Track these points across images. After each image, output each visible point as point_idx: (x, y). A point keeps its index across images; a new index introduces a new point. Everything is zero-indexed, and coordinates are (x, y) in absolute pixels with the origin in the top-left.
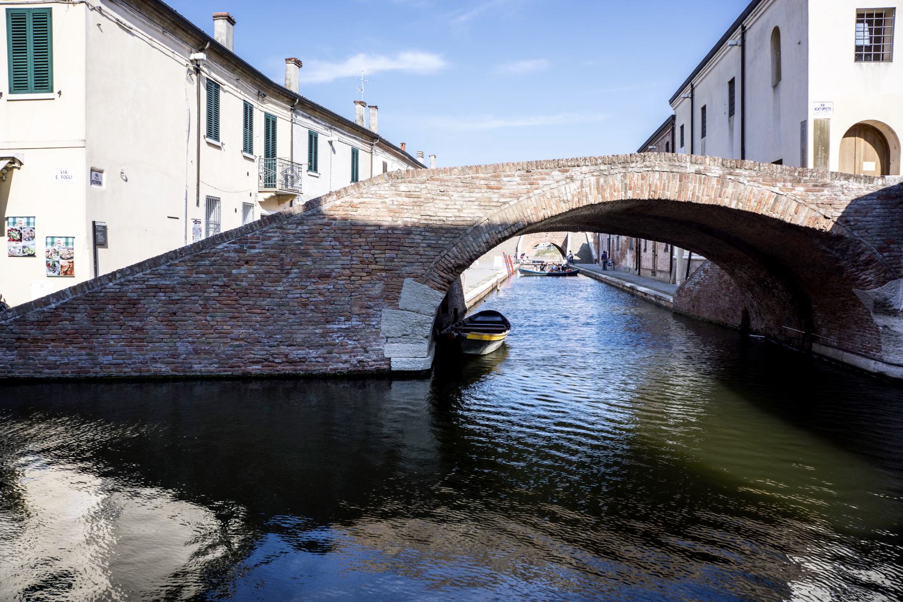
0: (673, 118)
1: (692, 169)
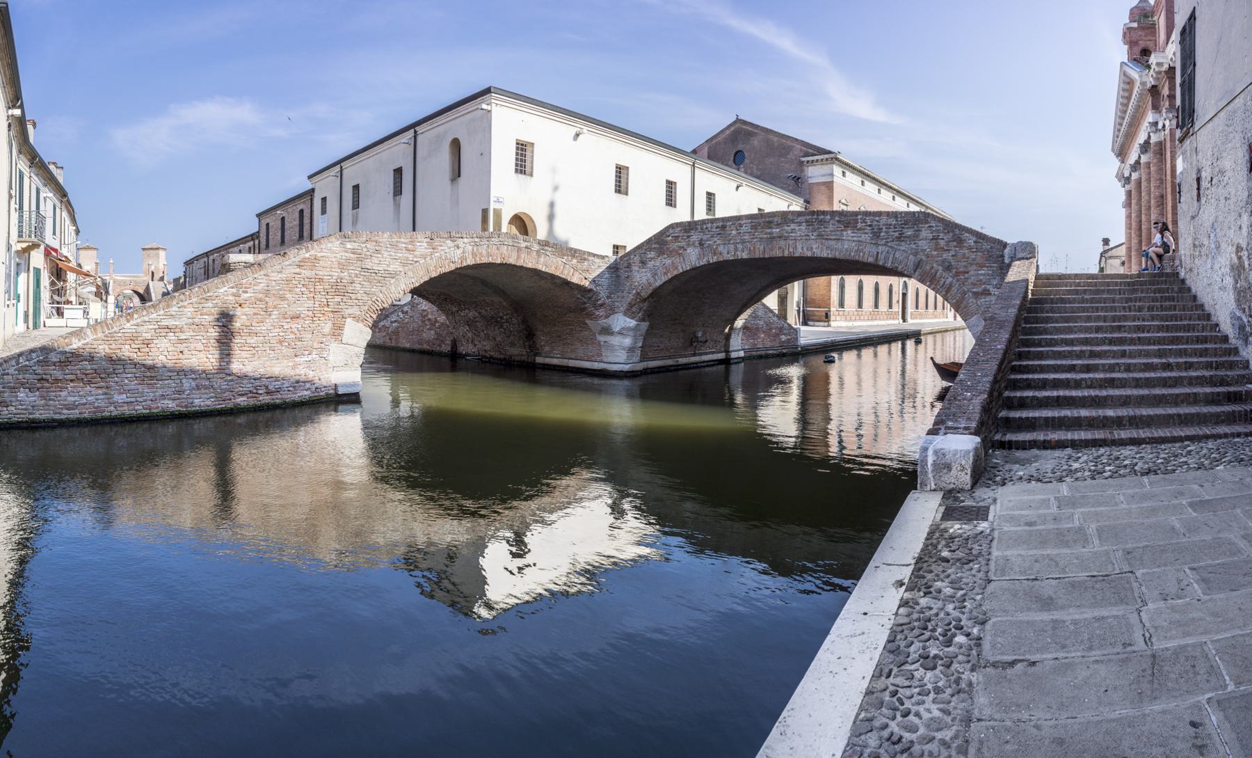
0: (313, 190)
1: (523, 245)
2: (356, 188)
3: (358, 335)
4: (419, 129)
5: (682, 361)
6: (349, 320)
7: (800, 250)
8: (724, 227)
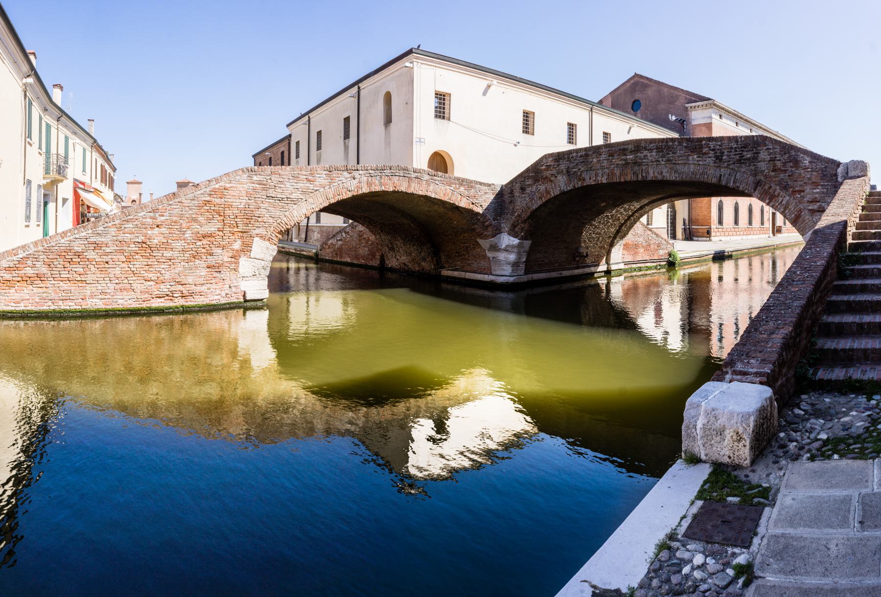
0: (290, 136)
1: (413, 175)
2: (319, 133)
3: (264, 251)
4: (360, 85)
5: (566, 273)
6: (256, 239)
8: (587, 155)
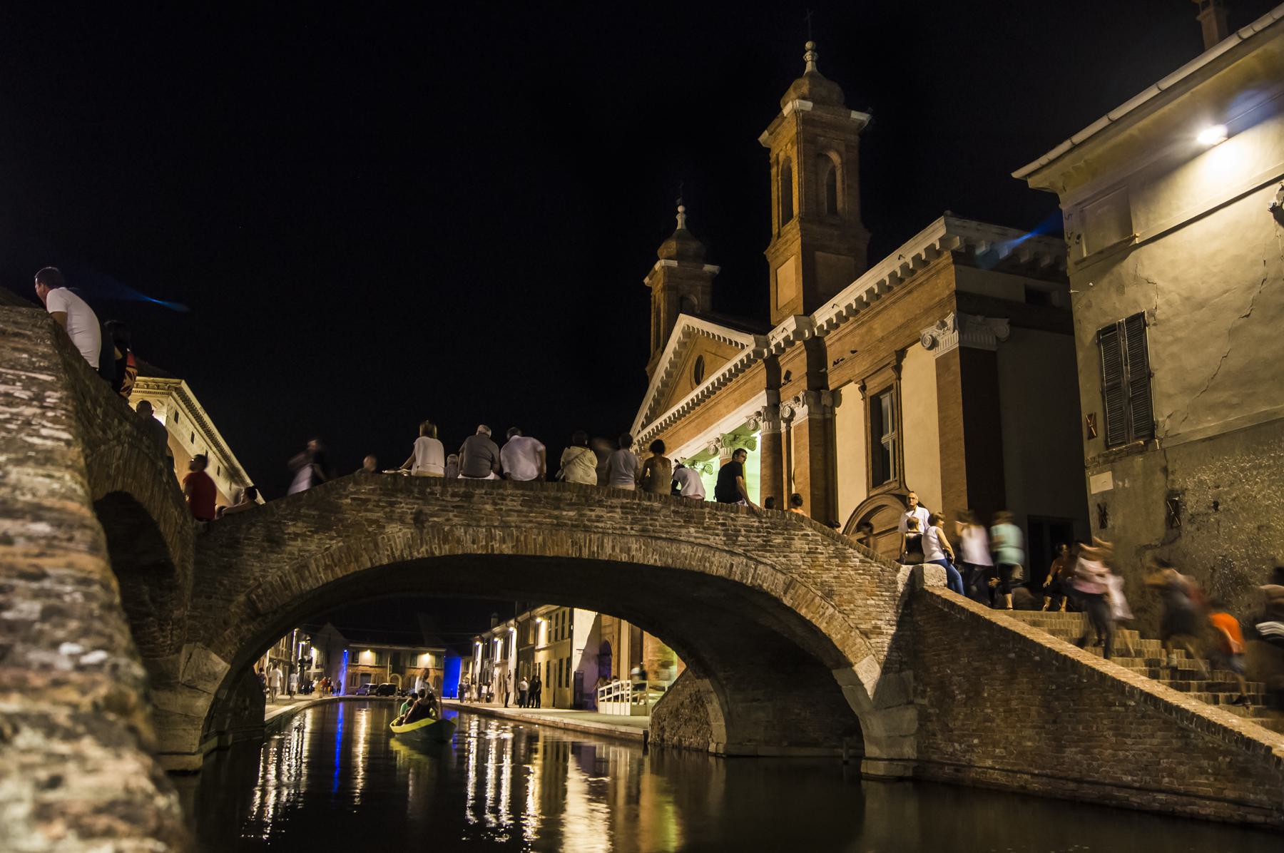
7: (608, 550)
